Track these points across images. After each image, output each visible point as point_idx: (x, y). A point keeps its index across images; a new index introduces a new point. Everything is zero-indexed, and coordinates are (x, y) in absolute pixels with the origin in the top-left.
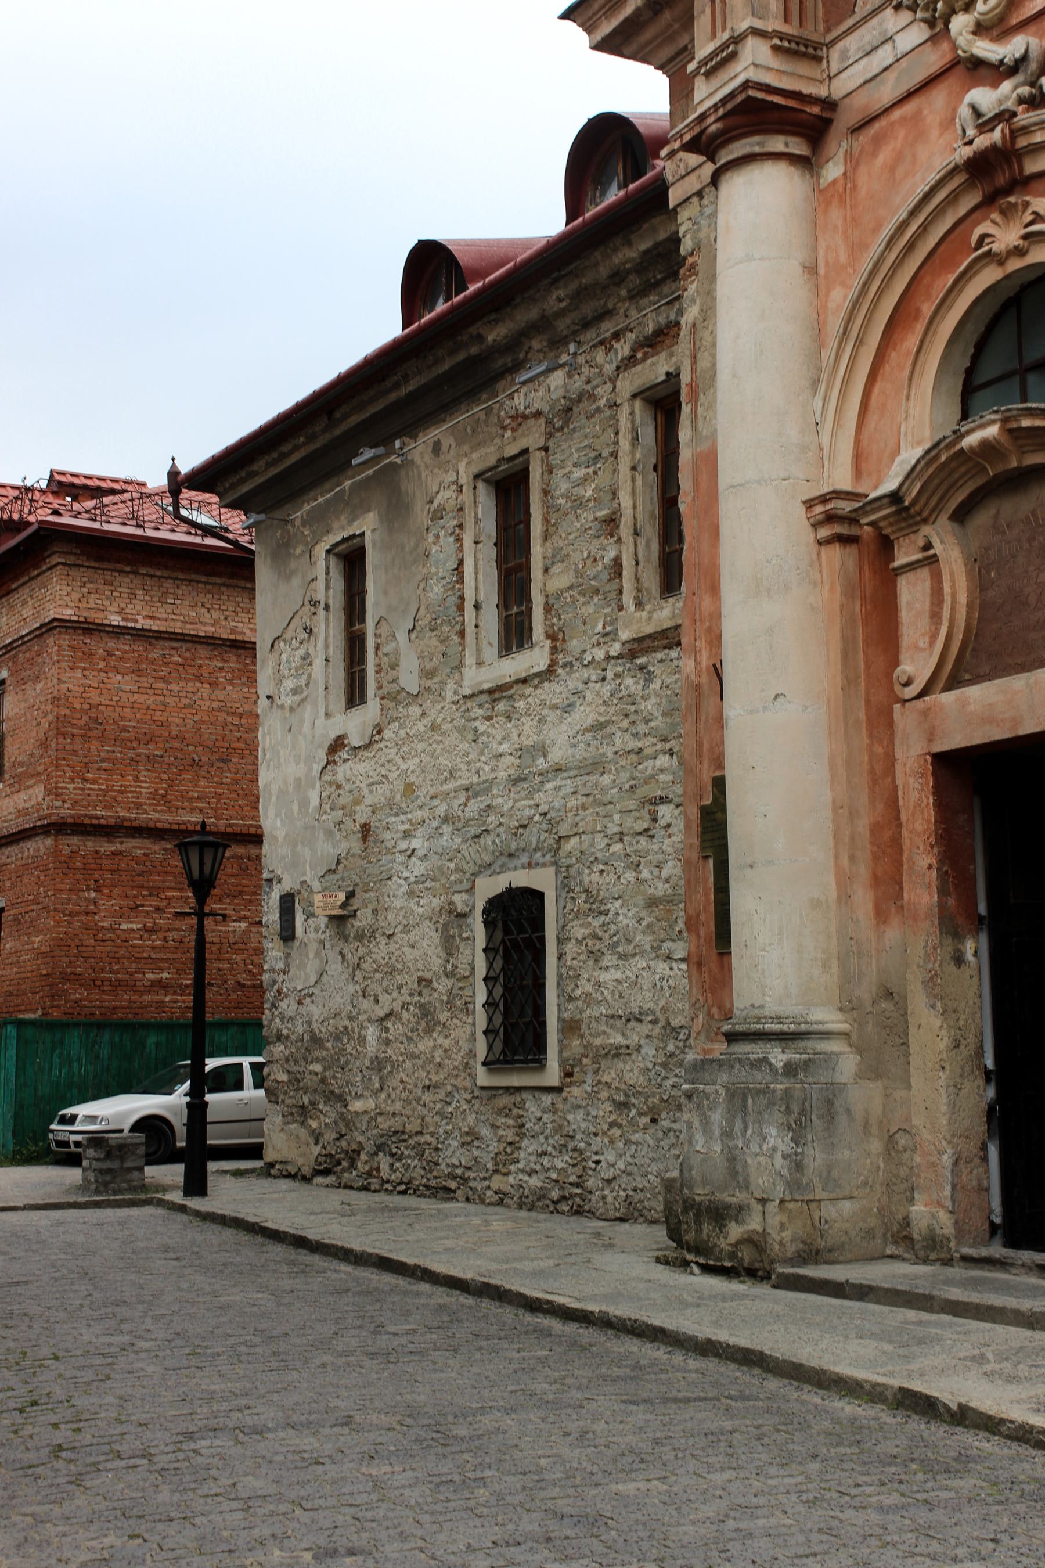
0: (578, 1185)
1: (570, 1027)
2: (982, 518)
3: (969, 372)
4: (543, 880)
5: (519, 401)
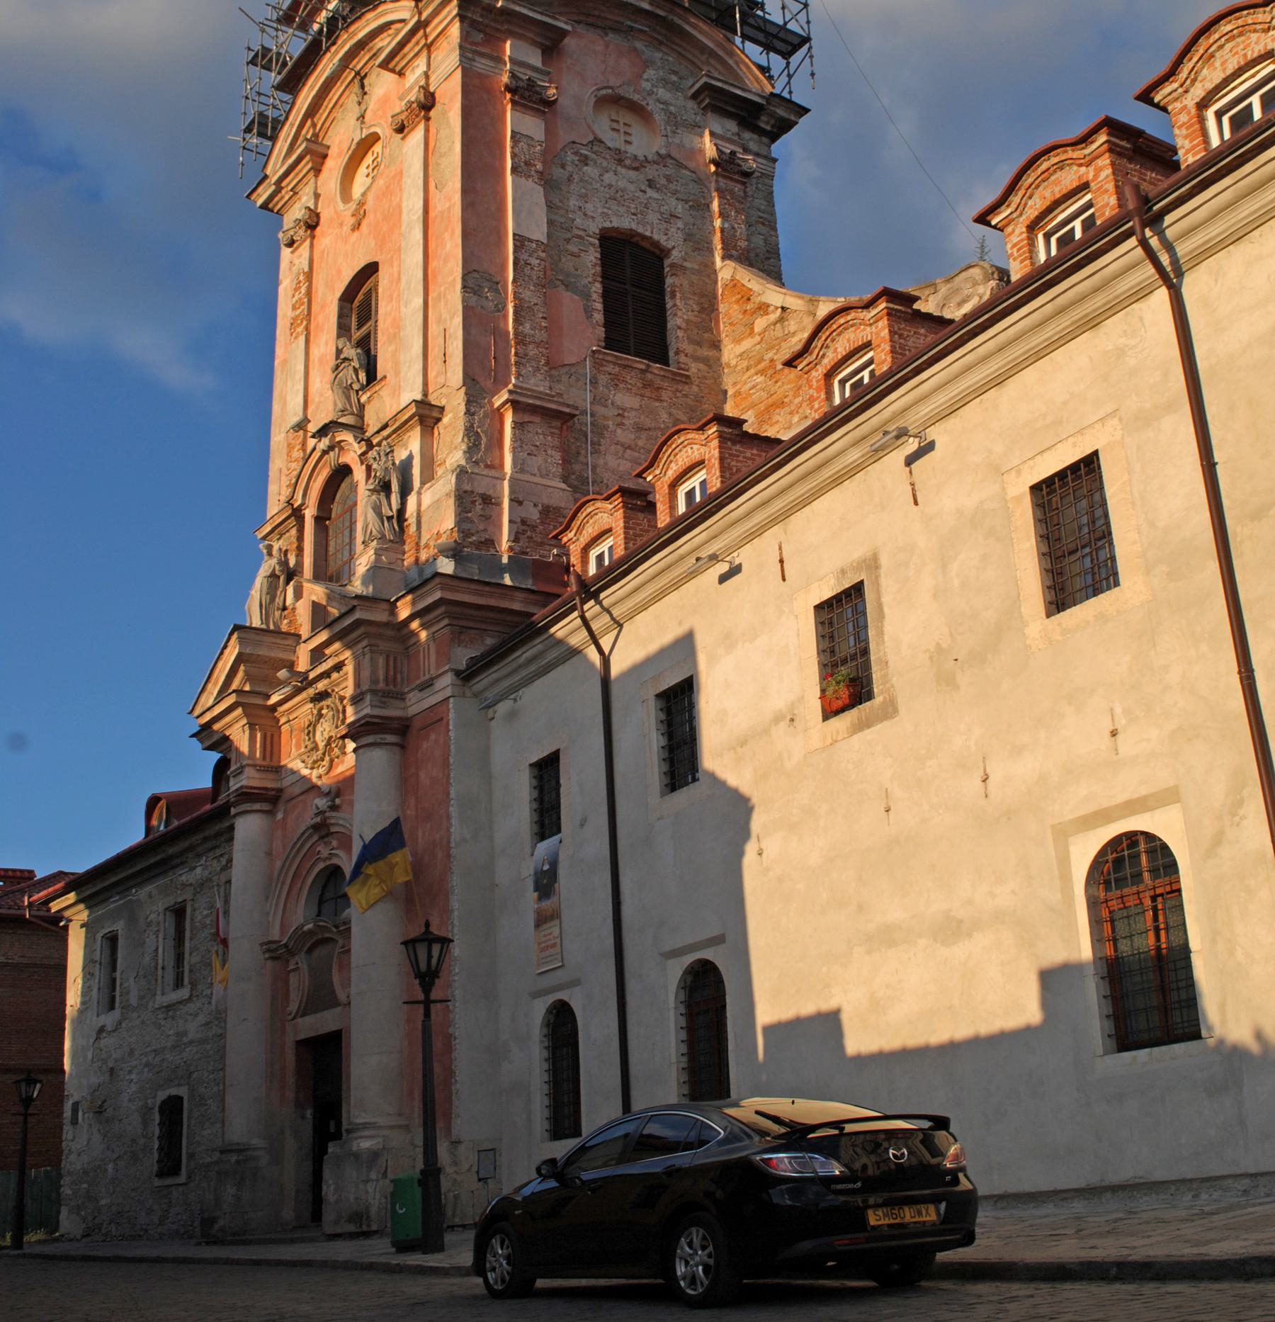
0: (191, 1225)
1: (191, 1156)
2: (316, 953)
3: (321, 896)
4: (183, 1091)
5: (184, 878)
